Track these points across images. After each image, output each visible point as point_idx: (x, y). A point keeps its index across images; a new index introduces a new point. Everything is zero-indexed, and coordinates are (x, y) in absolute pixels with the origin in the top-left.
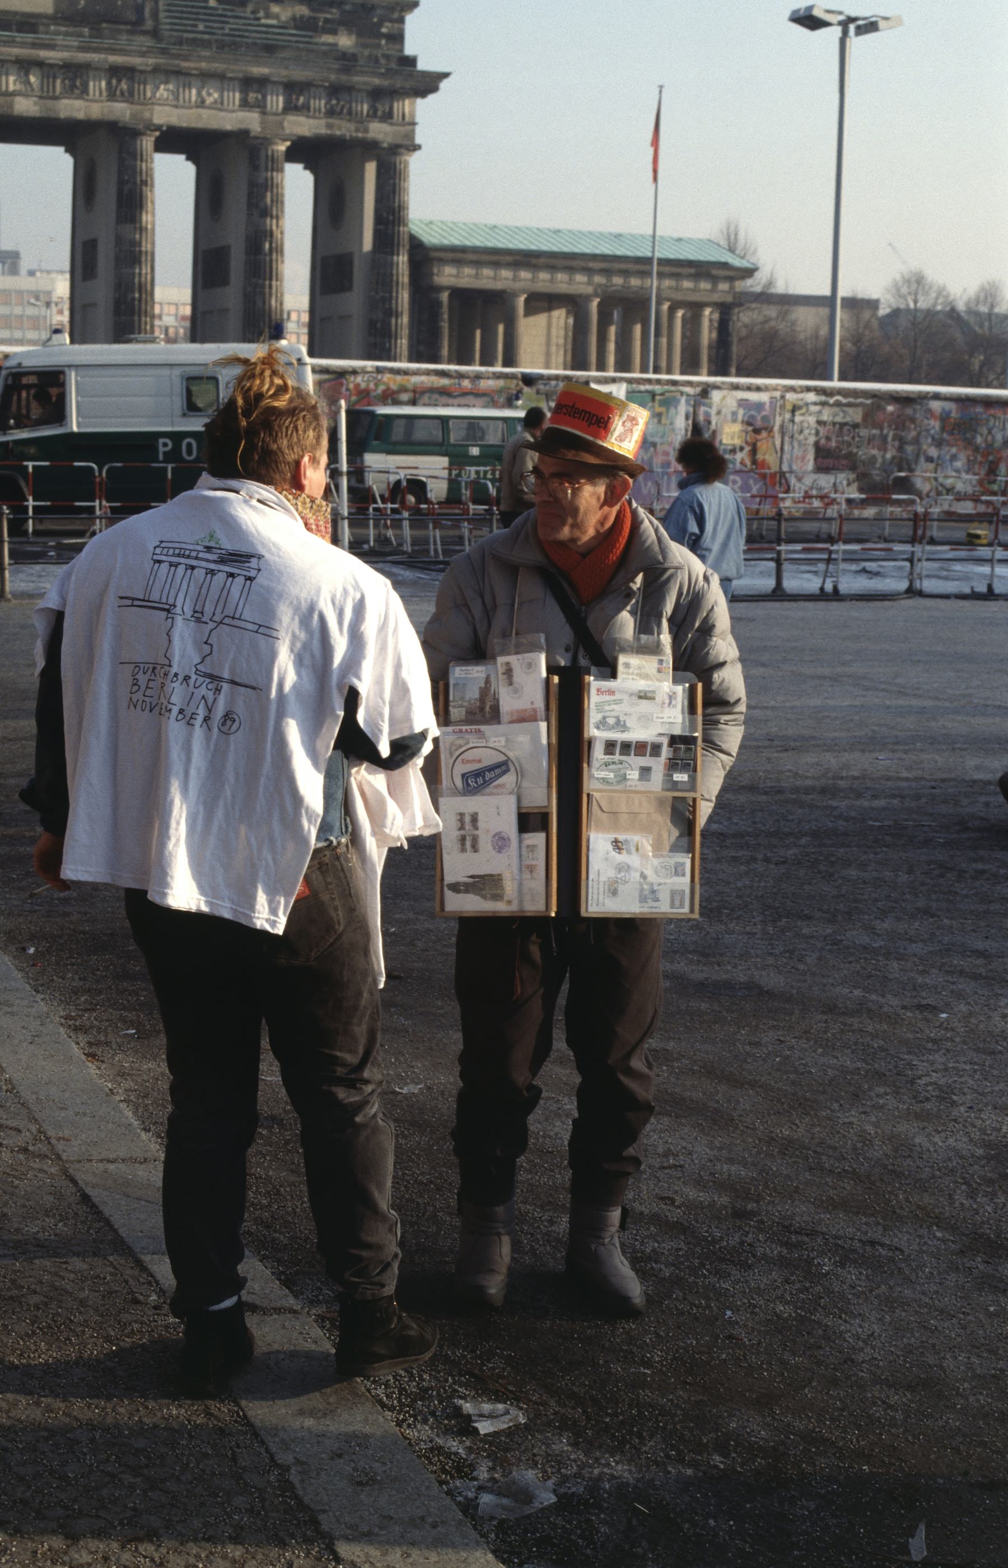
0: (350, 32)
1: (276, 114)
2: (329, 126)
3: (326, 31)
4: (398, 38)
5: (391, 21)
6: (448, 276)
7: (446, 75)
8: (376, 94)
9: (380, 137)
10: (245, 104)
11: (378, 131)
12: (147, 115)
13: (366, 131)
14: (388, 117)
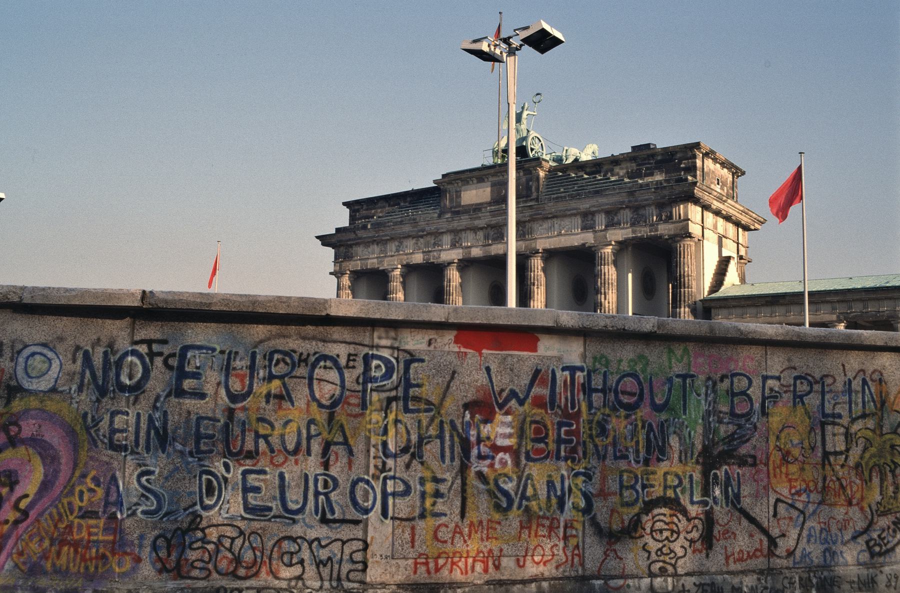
0: (661, 172)
1: (601, 231)
2: (634, 232)
3: (647, 175)
5: (687, 159)
10: (585, 228)
11: (665, 230)
12: (533, 245)
13: (657, 230)
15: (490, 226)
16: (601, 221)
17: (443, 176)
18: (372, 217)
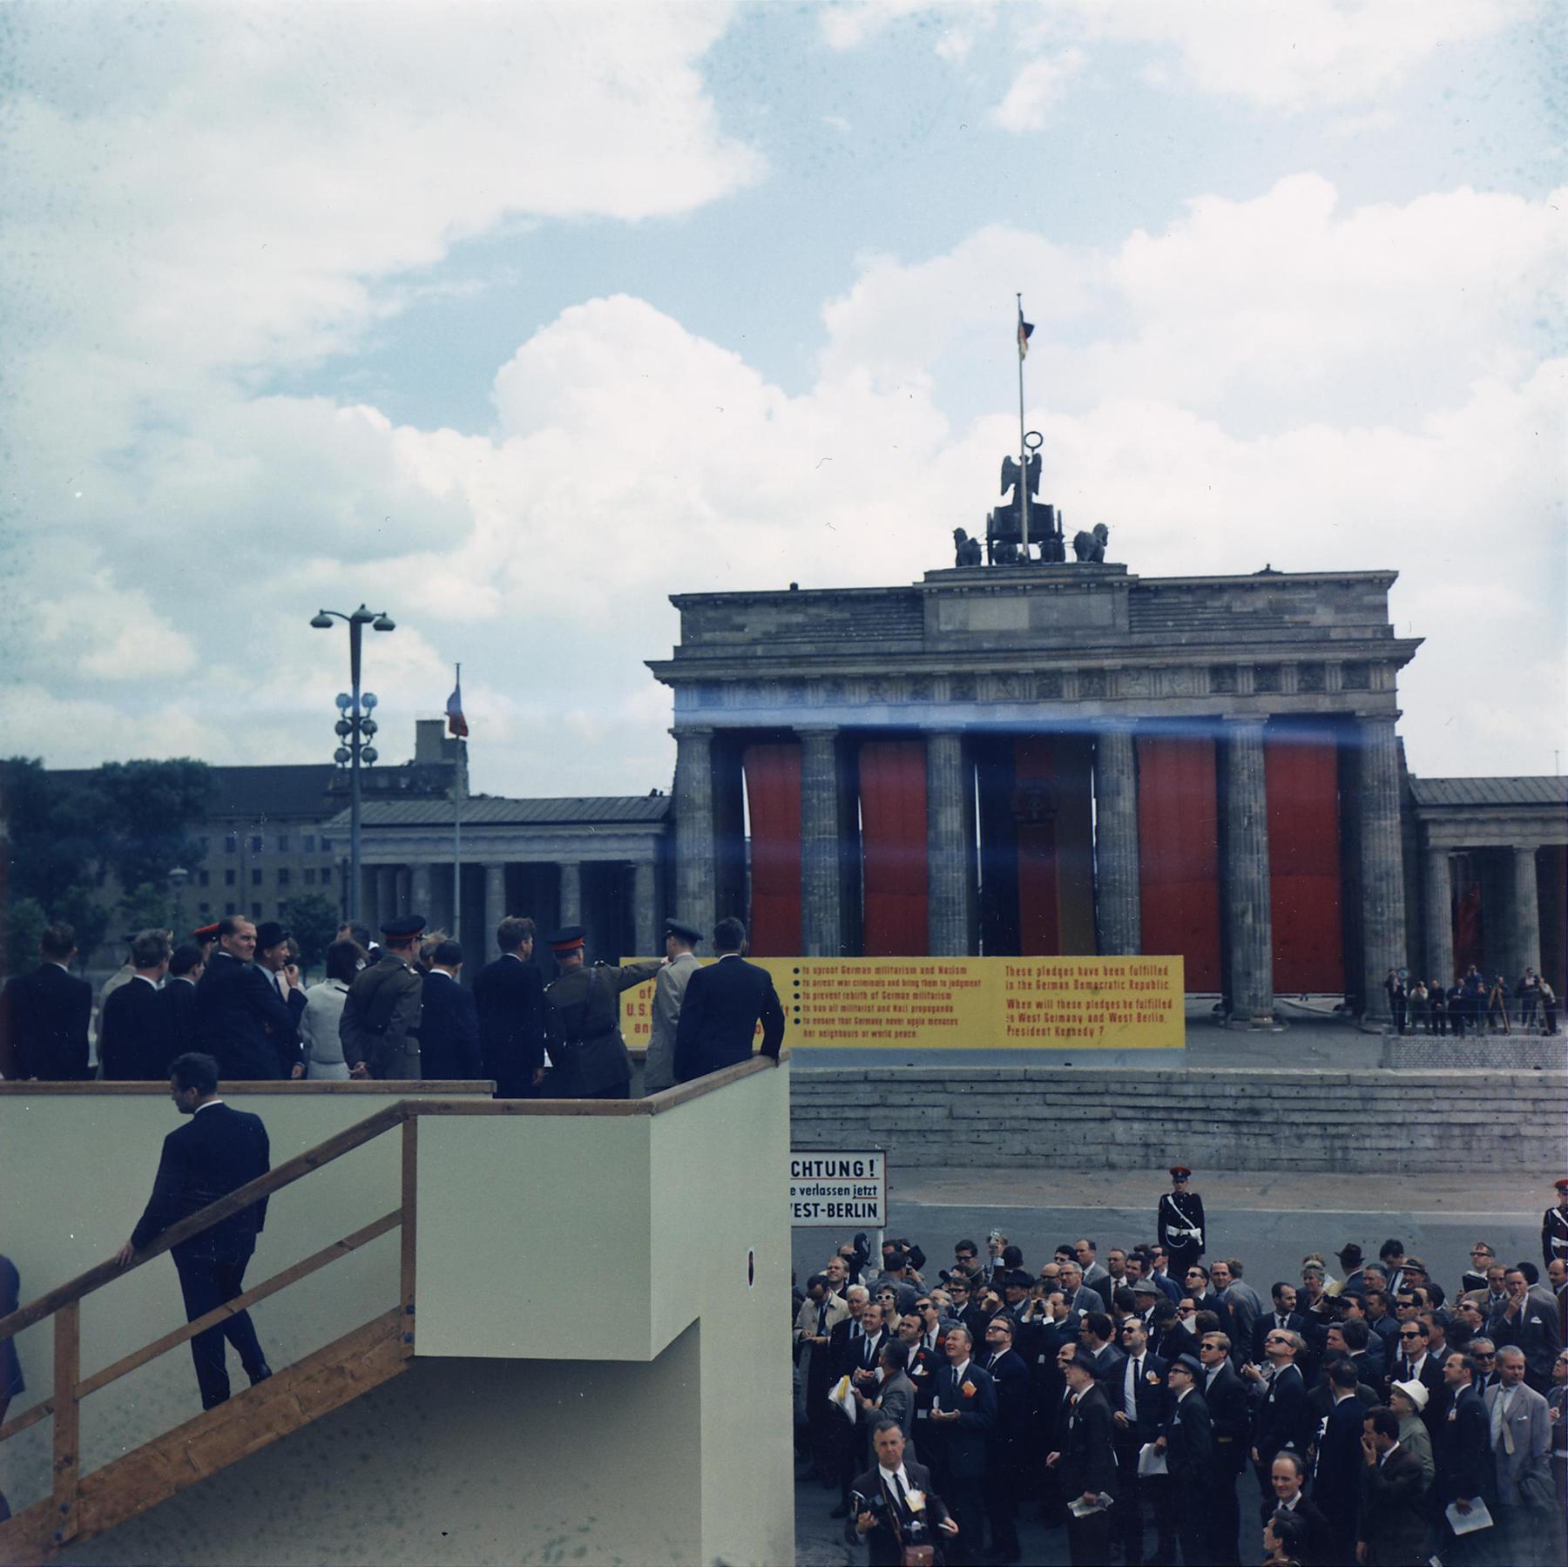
4: (1384, 607)
6: (1443, 837)
7: (1422, 640)
8: (1349, 667)
9: (1355, 707)
10: (1218, 690)
11: (1356, 701)
14: (1364, 686)
15: (1039, 674)
16: (1246, 683)
17: (930, 575)
18: (741, 628)
